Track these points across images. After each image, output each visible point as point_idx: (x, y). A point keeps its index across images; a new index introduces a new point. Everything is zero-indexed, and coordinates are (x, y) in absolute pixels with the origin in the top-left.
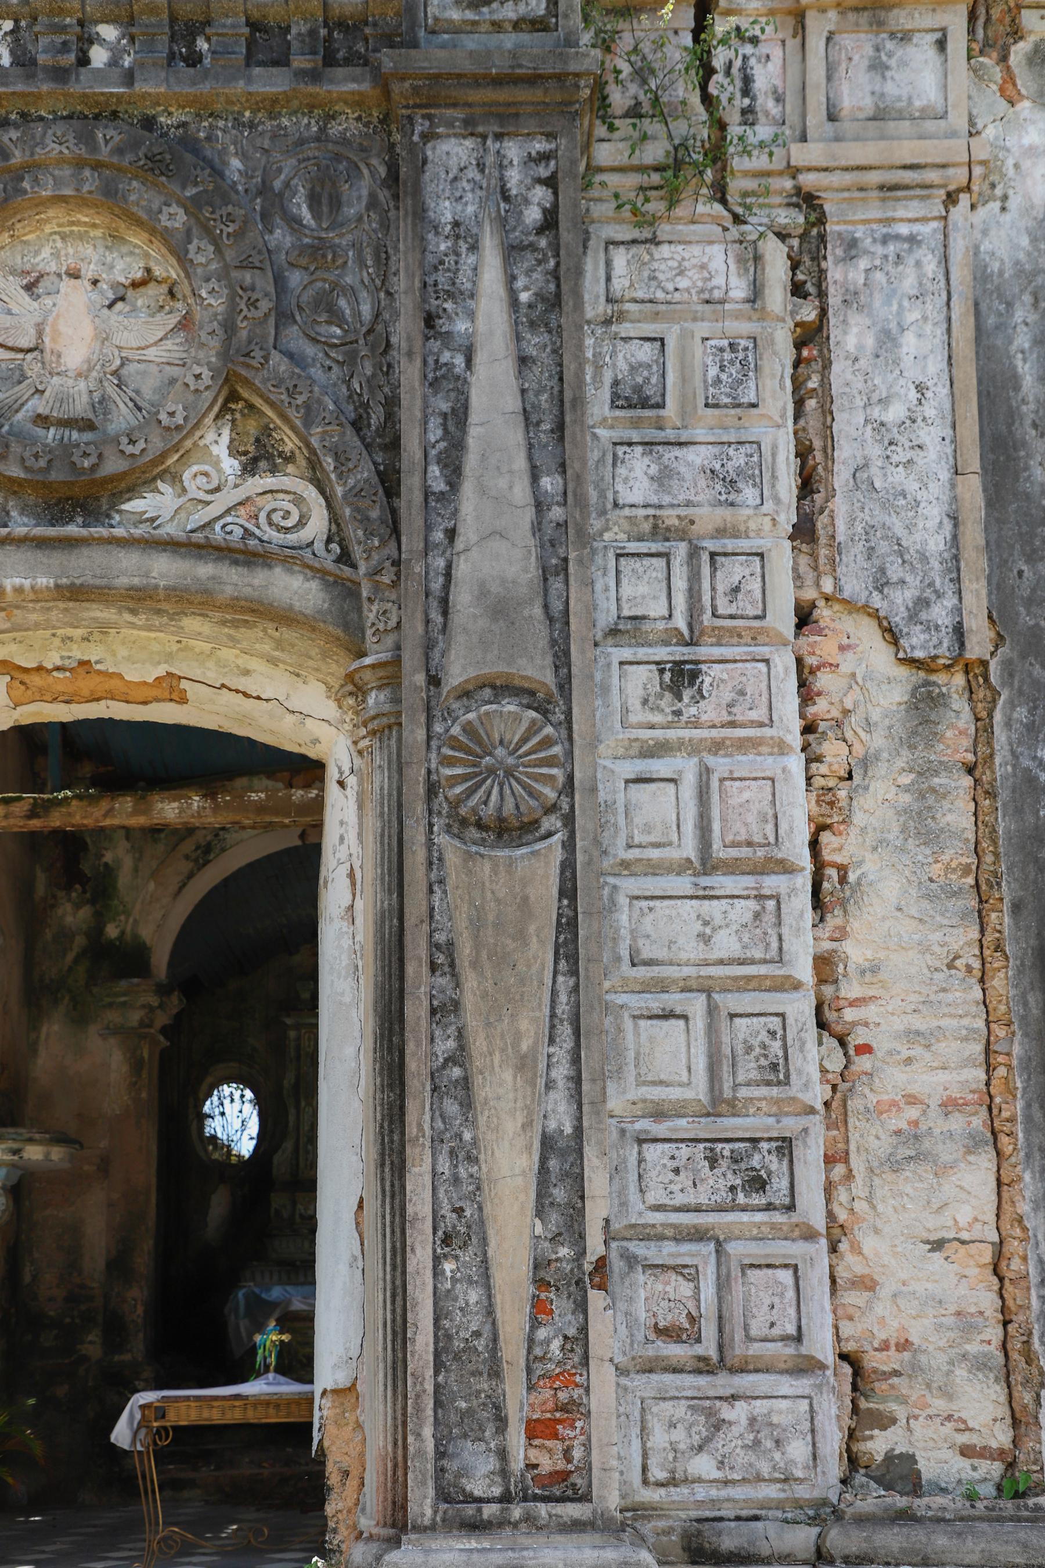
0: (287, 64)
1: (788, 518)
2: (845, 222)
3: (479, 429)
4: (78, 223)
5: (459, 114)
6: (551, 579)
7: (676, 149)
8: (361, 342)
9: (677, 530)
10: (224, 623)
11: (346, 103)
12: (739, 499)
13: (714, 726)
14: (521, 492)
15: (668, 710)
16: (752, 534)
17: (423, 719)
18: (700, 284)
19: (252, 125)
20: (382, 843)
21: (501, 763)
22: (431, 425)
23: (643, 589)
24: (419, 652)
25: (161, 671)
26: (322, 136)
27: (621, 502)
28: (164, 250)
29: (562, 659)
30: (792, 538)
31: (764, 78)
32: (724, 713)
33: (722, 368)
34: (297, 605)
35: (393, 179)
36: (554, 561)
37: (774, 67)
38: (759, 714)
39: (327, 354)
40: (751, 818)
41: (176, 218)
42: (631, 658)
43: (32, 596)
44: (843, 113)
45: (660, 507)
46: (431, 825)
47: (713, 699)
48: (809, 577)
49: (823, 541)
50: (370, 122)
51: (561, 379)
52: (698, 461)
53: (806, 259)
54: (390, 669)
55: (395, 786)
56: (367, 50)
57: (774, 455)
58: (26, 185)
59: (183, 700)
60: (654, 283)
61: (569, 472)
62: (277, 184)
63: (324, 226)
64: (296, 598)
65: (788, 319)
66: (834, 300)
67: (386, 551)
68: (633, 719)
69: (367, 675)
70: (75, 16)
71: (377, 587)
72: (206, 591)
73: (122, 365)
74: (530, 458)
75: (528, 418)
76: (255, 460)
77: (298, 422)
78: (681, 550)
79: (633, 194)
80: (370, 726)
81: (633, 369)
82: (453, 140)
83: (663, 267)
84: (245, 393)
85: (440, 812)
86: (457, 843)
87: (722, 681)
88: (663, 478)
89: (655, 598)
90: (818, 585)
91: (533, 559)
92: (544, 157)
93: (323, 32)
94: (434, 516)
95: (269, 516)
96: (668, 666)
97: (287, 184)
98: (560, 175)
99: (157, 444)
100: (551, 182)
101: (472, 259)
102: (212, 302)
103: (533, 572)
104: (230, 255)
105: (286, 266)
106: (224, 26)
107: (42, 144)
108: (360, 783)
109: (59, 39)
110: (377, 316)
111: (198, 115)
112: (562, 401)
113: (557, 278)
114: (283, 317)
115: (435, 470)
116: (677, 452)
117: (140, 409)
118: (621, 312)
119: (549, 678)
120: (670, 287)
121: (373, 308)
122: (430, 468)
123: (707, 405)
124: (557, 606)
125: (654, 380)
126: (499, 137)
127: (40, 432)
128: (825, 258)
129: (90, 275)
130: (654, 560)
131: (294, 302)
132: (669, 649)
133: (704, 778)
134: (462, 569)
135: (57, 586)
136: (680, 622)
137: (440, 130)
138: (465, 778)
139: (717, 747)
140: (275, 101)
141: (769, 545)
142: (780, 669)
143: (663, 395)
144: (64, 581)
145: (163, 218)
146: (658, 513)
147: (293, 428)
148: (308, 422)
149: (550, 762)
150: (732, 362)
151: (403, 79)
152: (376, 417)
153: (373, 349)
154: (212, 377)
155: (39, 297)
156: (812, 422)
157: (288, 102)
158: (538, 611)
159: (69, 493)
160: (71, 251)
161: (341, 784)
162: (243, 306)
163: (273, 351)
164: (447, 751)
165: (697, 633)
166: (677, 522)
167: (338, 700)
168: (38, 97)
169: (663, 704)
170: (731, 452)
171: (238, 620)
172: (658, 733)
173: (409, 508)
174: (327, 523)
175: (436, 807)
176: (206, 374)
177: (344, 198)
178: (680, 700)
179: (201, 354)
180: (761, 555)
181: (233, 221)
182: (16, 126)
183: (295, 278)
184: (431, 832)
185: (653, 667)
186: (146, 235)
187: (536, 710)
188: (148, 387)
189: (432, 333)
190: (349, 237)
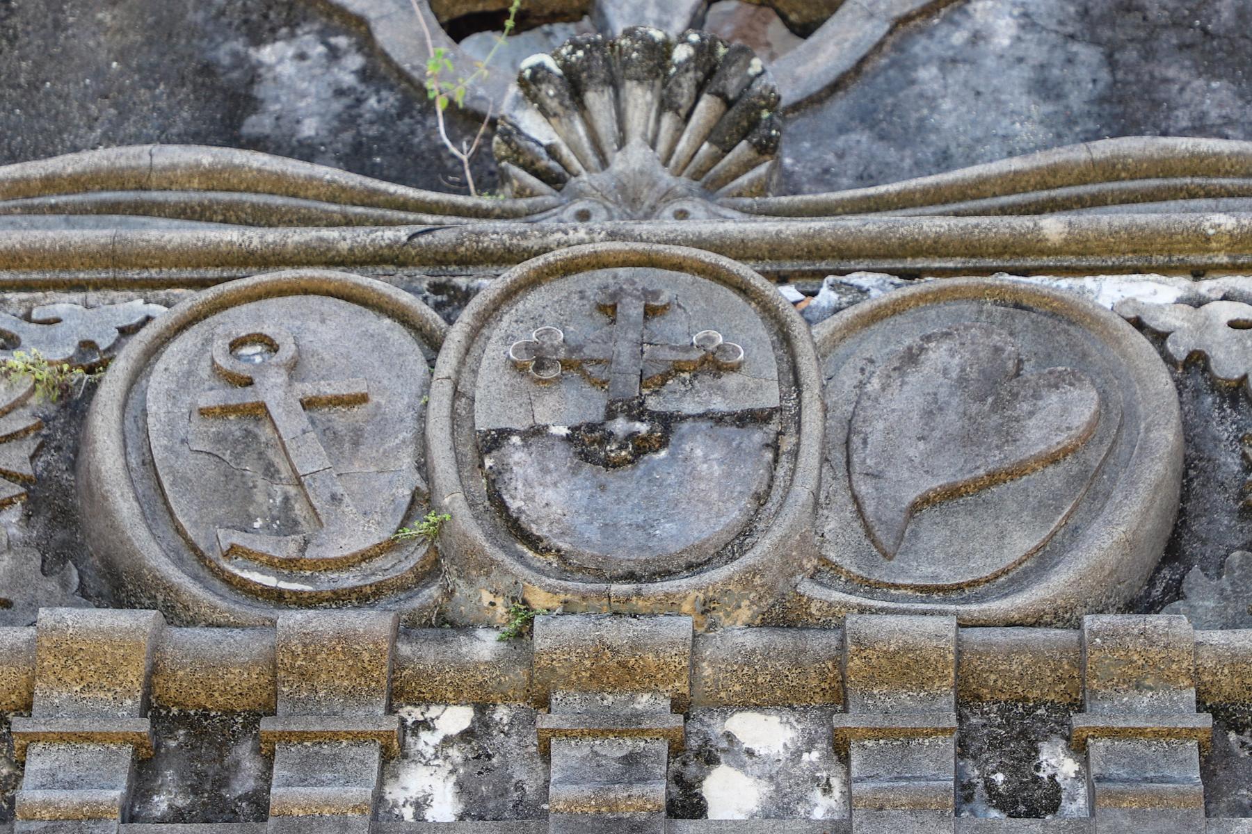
70: (667, 690)
109: (613, 750)
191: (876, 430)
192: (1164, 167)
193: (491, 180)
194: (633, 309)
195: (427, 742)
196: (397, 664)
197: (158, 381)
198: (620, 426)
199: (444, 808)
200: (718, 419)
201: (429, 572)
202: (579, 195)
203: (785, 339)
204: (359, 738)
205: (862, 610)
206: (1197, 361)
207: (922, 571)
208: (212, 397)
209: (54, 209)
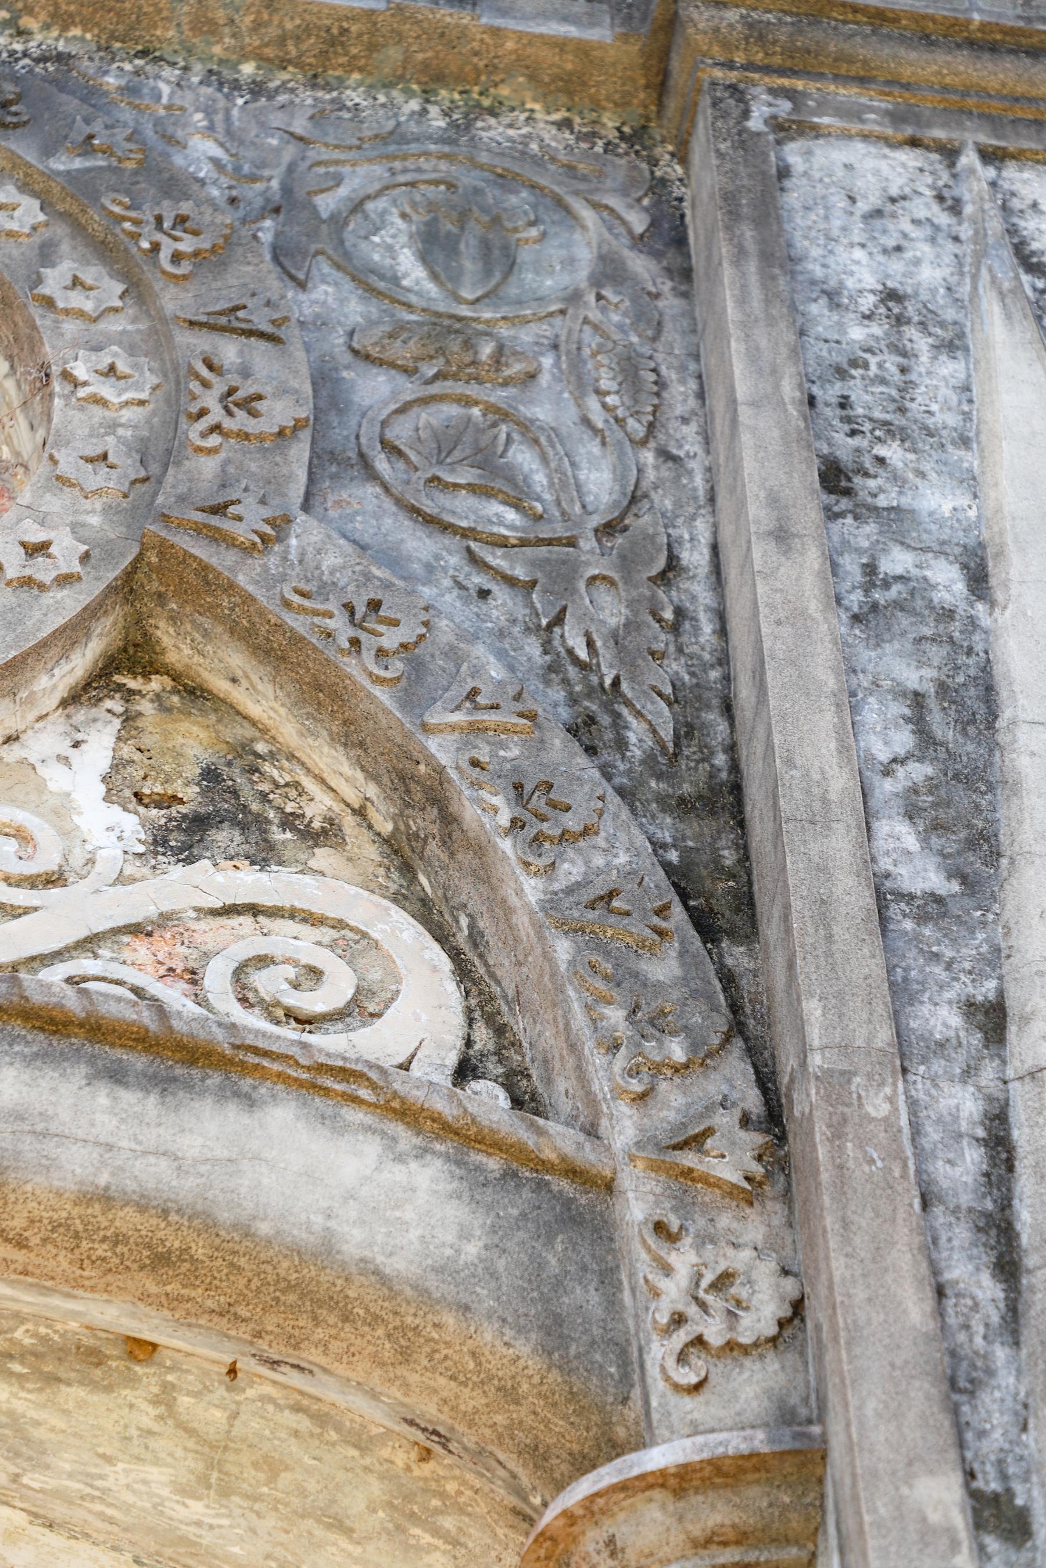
39: (473, 559)
50: (594, 134)
62: (327, 203)
63: (467, 294)
64: (352, 1211)
77: (381, 694)
95: (240, 972)
97: (357, 206)
101: (950, 368)
105: (347, 358)
110: (634, 500)
121: (620, 476)
122: (882, 828)
131: (369, 435)
154: (85, 558)
157: (372, 47)
162: (211, 400)
163: (302, 518)
177: (525, 255)
181: (196, 233)
189: (844, 504)
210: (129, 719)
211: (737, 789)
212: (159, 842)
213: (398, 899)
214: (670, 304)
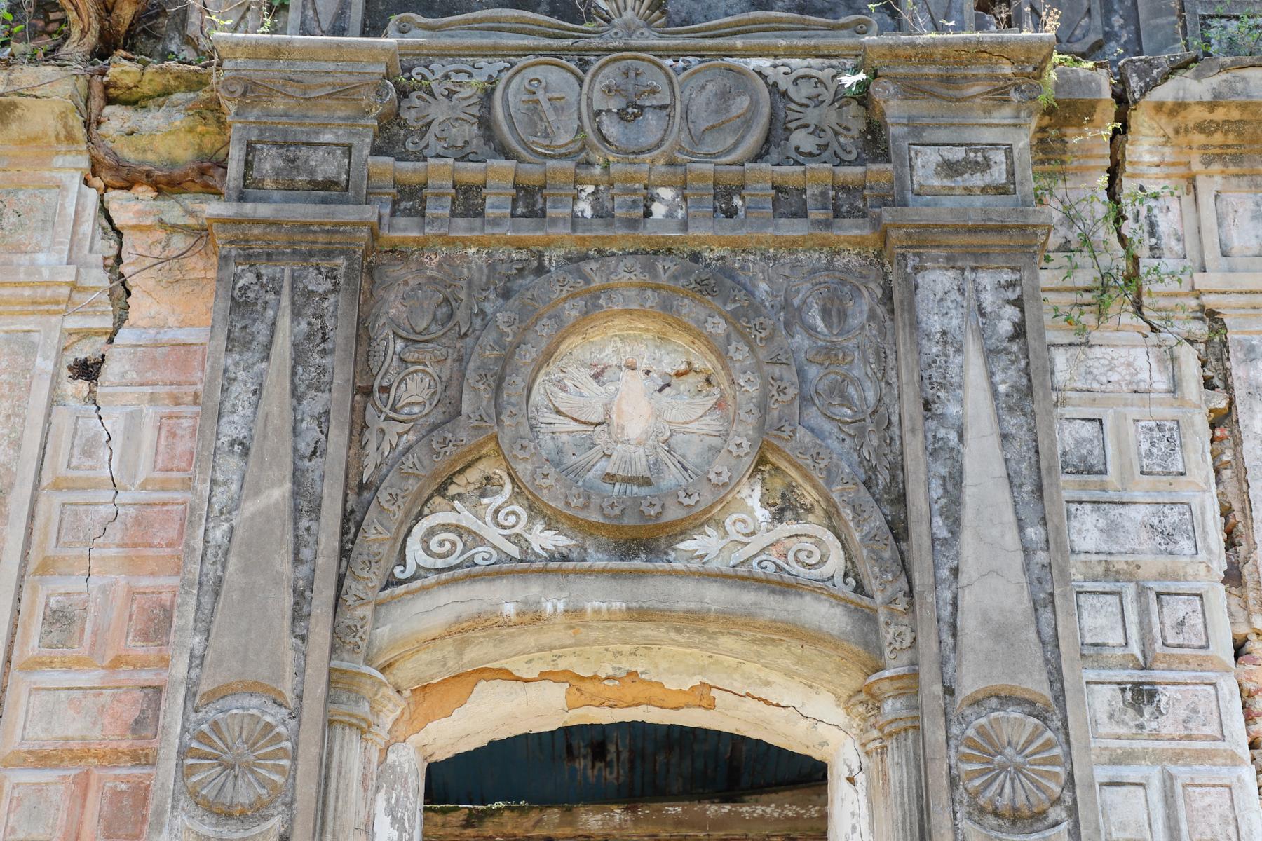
0: (806, 216)
1: (1220, 566)
2: (1243, 333)
3: (973, 489)
4: (635, 328)
5: (942, 253)
6: (1041, 610)
7: (1103, 276)
8: (868, 420)
9: (1125, 573)
10: (754, 641)
11: (849, 243)
12: (1177, 549)
13: (1173, 739)
14: (1011, 539)
15: (1132, 724)
16: (1190, 578)
17: (942, 722)
18: (1128, 378)
19: (775, 259)
20: (904, 829)
21: (1011, 761)
22: (933, 485)
23: (1101, 621)
24: (935, 667)
25: (695, 681)
26: (830, 267)
27: (1076, 549)
28: (704, 349)
29: (1056, 675)
30: (1224, 582)
31: (1165, 224)
32: (1181, 727)
33: (1153, 444)
34: (825, 627)
35: (888, 297)
36: (1042, 595)
37: (1174, 215)
38: (1212, 729)
40: (1214, 820)
41: (718, 327)
42: (1095, 678)
43: (606, 617)
44: (1233, 251)
45: (1110, 554)
46: (955, 813)
47: (1170, 715)
48: (1241, 615)
49: (1250, 585)
51: (1037, 452)
52: (1139, 518)
53: (1212, 359)
54: (906, 682)
55: (913, 780)
56: (865, 205)
57: (1203, 514)
58: (602, 302)
59: (711, 706)
60: (1090, 377)
61: (1050, 525)
65: (1203, 406)
66: (1239, 392)
67: (898, 585)
68: (1102, 730)
69: (886, 686)
71: (892, 613)
72: (749, 615)
73: (671, 435)
74: (1016, 513)
75: (1012, 481)
76: (782, 510)
77: (821, 481)
78: (1130, 590)
79: (1067, 309)
80: (887, 730)
81: (1079, 443)
82: (938, 271)
83: (1096, 364)
84: (772, 458)
85: (961, 802)
86: (977, 827)
87: (1177, 700)
88: (1110, 530)
89: (1112, 629)
90: (1249, 621)
91: (1026, 593)
92: (1011, 285)
93: (831, 193)
94: (940, 557)
96: (1129, 686)
97: (804, 302)
98: (1025, 298)
99: (707, 497)
100: (1018, 303)
101: (958, 359)
102: (748, 388)
103: (1027, 604)
104: (762, 354)
106: (756, 189)
107: (615, 272)
108: (869, 780)
109: (630, 198)
111: (733, 251)
112: (1039, 469)
113: (1028, 375)
114: (805, 400)
115: (938, 521)
116: (1120, 509)
117: (686, 470)
118: (1064, 399)
119: (1046, 691)
120: (1104, 380)
122: (934, 519)
123: (1142, 473)
124: (1048, 632)
125: (1096, 452)
126: (974, 269)
127: (608, 487)
128: (1228, 359)
129: (644, 367)
130: (1109, 597)
131: (813, 389)
132: (1127, 672)
133: (1168, 784)
134: (966, 601)
135: (628, 609)
136: (1135, 649)
137: (928, 264)
138: (982, 773)
139: (1177, 757)
140: (795, 241)
141: (1206, 588)
142: (1226, 691)
143: (1105, 464)
144: (634, 604)
145: (709, 326)
146: (1109, 558)
147: (815, 486)
148: (829, 482)
149: (1053, 761)
150: (1160, 439)
151: (899, 228)
152: (883, 478)
153: (878, 425)
155: (604, 384)
156: (1231, 489)
158: (1033, 635)
159: (635, 535)
160: (628, 349)
161: (851, 780)
162: (774, 392)
164: (963, 749)
165: (1150, 659)
166: (1125, 567)
167: (846, 709)
168: (614, 239)
169: (1127, 718)
170: (1166, 510)
171: (767, 639)
172: (1125, 743)
173: (920, 550)
174: (843, 561)
175: (957, 797)
176: (746, 443)
177: (849, 312)
178: (1142, 716)
179: (741, 428)
180: (1200, 596)
182: (596, 260)
183: (813, 372)
184: (955, 819)
185: (1116, 687)
186: (691, 338)
187: (1036, 717)
188: (692, 452)
190: (855, 341)
191: (694, 109)
192: (768, 21)
193: (590, 18)
194: (632, 74)
195: (583, 195)
196: (576, 174)
197: (511, 91)
198: (630, 110)
199: (588, 213)
200: (654, 107)
201: (583, 149)
202: (614, 27)
203: (671, 82)
204: (567, 195)
205: (691, 162)
206: (775, 84)
207: (705, 149)
208: (525, 98)
209: (477, 29)
210: (763, 480)
211: (904, 495)
212: (774, 518)
213: (828, 527)
214: (888, 324)
